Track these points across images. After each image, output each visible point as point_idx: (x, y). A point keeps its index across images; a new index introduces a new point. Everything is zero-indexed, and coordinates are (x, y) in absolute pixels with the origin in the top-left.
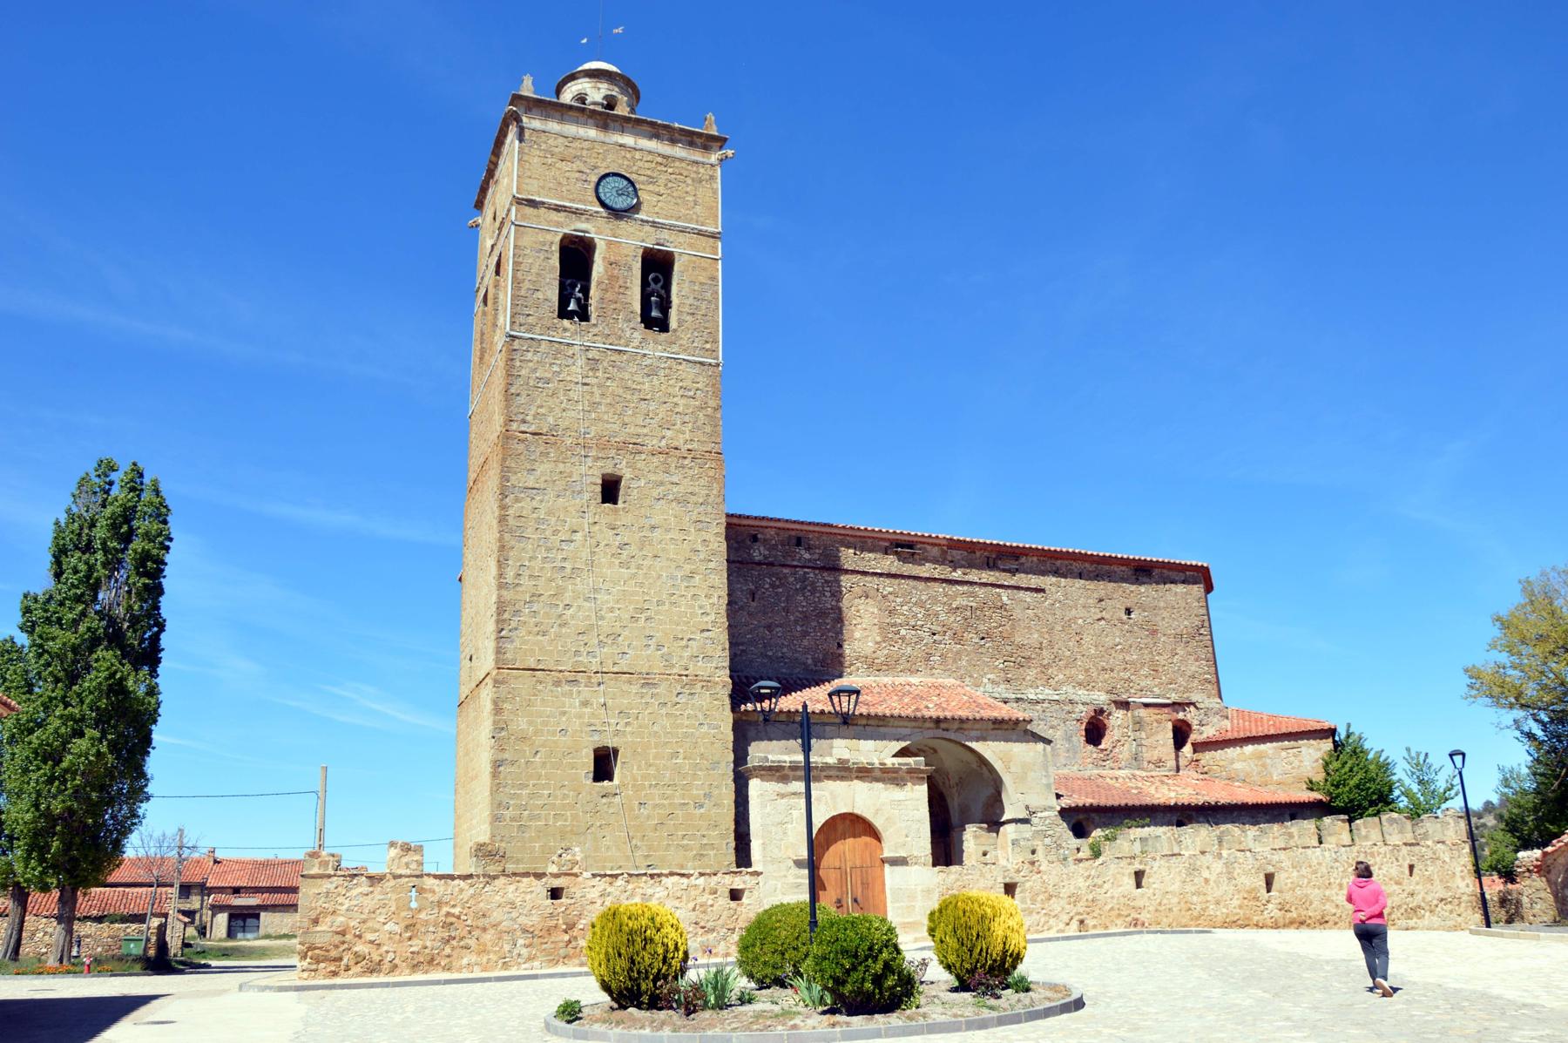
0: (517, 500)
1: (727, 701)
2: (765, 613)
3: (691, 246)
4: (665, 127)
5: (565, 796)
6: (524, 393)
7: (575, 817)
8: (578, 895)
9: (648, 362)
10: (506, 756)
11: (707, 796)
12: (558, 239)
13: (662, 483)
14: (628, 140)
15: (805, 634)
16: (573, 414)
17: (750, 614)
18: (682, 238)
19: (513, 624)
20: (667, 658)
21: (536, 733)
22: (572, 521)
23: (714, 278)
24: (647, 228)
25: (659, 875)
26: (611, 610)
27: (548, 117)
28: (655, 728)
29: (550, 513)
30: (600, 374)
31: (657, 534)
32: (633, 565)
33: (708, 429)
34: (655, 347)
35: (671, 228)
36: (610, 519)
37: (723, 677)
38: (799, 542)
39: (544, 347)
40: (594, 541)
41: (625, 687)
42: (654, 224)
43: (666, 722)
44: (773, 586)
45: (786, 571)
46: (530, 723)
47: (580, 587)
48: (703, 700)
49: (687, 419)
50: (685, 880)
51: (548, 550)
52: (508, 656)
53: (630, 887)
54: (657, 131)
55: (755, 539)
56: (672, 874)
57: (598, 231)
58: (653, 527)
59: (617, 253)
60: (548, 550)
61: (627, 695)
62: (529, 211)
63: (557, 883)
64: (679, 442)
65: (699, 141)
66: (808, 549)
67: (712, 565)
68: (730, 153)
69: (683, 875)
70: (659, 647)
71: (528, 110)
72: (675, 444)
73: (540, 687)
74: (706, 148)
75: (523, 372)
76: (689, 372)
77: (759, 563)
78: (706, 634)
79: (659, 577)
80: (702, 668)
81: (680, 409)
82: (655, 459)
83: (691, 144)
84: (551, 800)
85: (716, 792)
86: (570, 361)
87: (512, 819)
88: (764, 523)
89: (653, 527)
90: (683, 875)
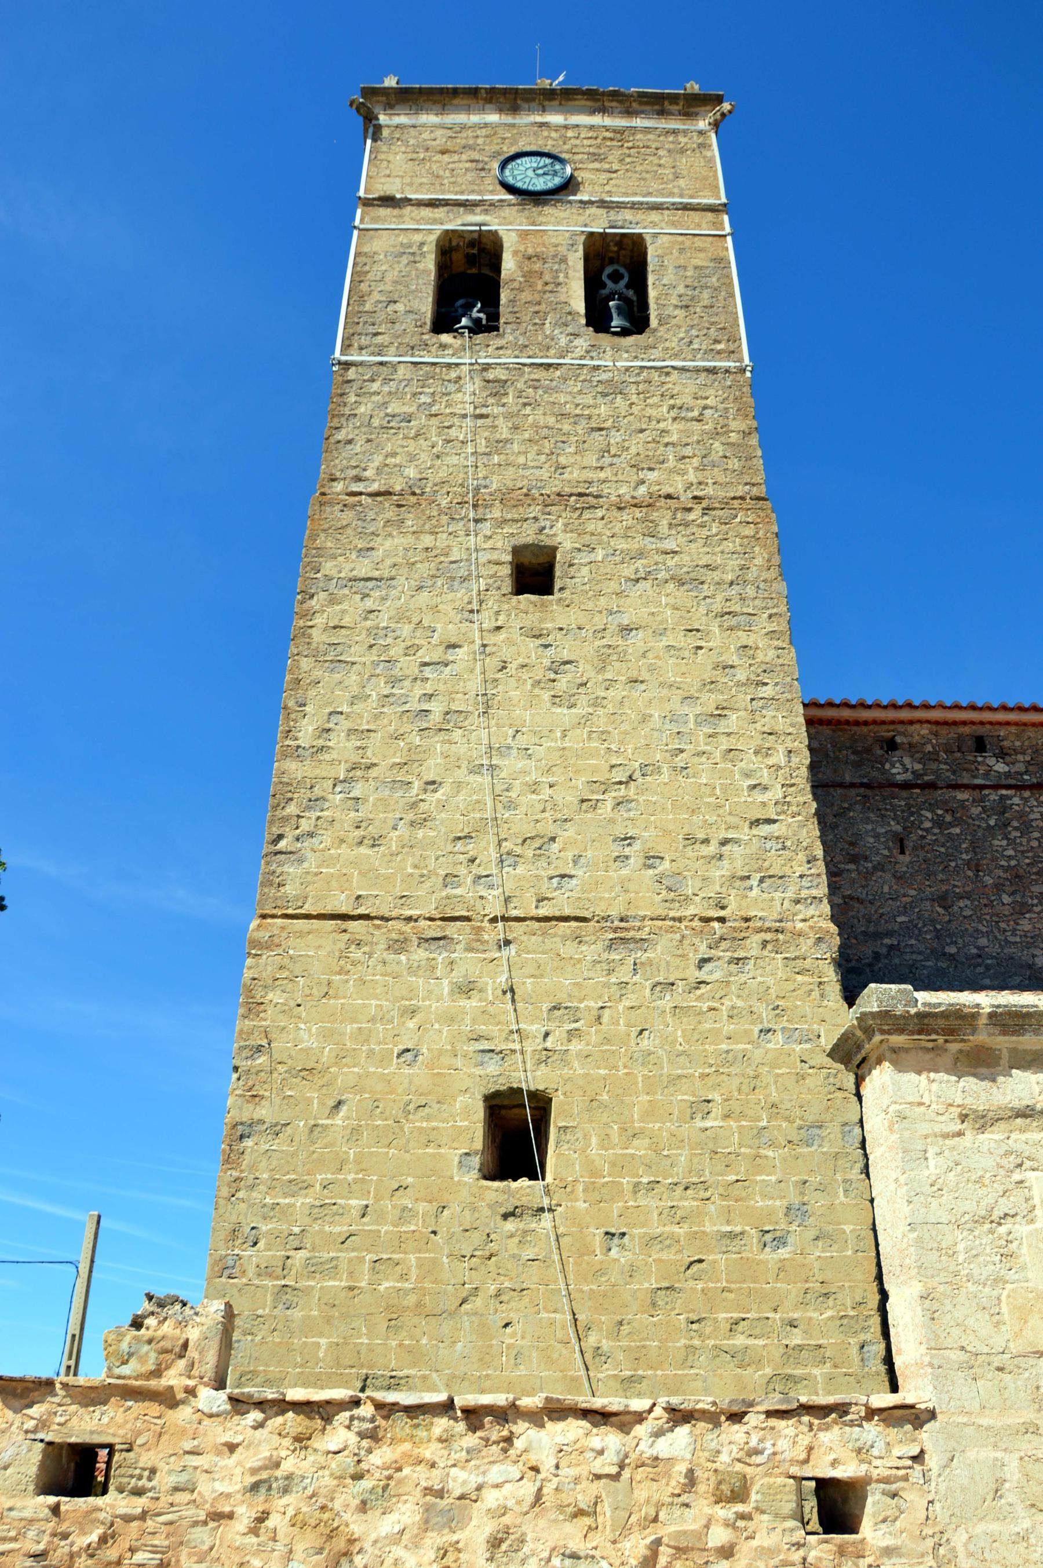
0: (333, 601)
1: (831, 975)
2: (930, 874)
3: (673, 224)
4: (615, 95)
5: (405, 1214)
6: (360, 441)
7: (429, 1269)
8: (165, 1480)
9: (604, 377)
10: (263, 1112)
11: (796, 1212)
12: (433, 238)
13: (641, 554)
14: (556, 119)
15: (1022, 909)
16: (454, 460)
17: (899, 878)
18: (654, 216)
19: (305, 825)
20: (671, 887)
21: (339, 1058)
22: (446, 628)
23: (721, 261)
24: (593, 210)
25: (504, 1414)
26: (534, 788)
27: (420, 110)
28: (645, 1043)
29: (401, 617)
30: (510, 399)
31: (637, 639)
32: (583, 700)
33: (734, 464)
34: (618, 355)
35: (633, 206)
36: (531, 620)
37: (816, 918)
38: (980, 745)
39: (401, 370)
40: (492, 663)
41: (569, 949)
42: (603, 204)
43: (677, 1029)
44: (939, 823)
45: (962, 795)
46: (327, 1035)
47: (461, 749)
48: (769, 973)
49: (688, 451)
50: (610, 1439)
51: (394, 681)
52: (290, 889)
53: (380, 1457)
54: (598, 100)
55: (891, 745)
56: (557, 1411)
57: (510, 226)
58: (626, 630)
59: (544, 252)
60: (394, 681)
61: (569, 969)
62: (383, 212)
63: (84, 1426)
64: (676, 486)
65: (674, 108)
66: (1002, 755)
67: (767, 691)
69: (600, 1417)
70: (651, 859)
71: (389, 106)
72: (667, 489)
73: (357, 954)
74: (688, 114)
75: (362, 409)
76: (685, 389)
77: (906, 786)
78: (765, 829)
79: (645, 719)
80: (762, 903)
81: (674, 438)
82: (625, 515)
83: (662, 113)
84: (368, 1225)
85: (818, 1202)
86: (452, 387)
87: (265, 1271)
88: (905, 714)
89: (626, 630)
90: (600, 1417)
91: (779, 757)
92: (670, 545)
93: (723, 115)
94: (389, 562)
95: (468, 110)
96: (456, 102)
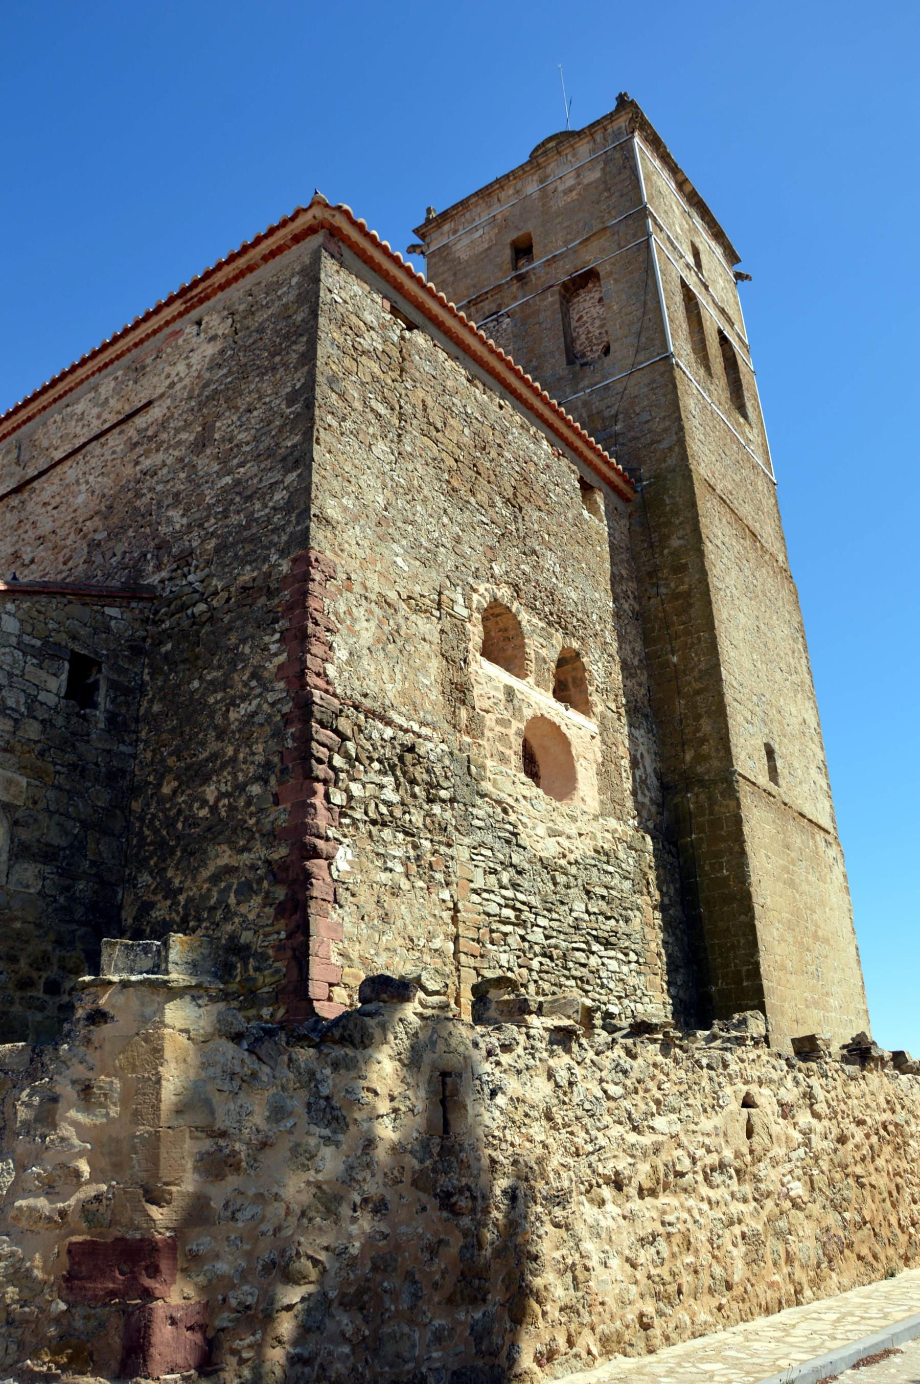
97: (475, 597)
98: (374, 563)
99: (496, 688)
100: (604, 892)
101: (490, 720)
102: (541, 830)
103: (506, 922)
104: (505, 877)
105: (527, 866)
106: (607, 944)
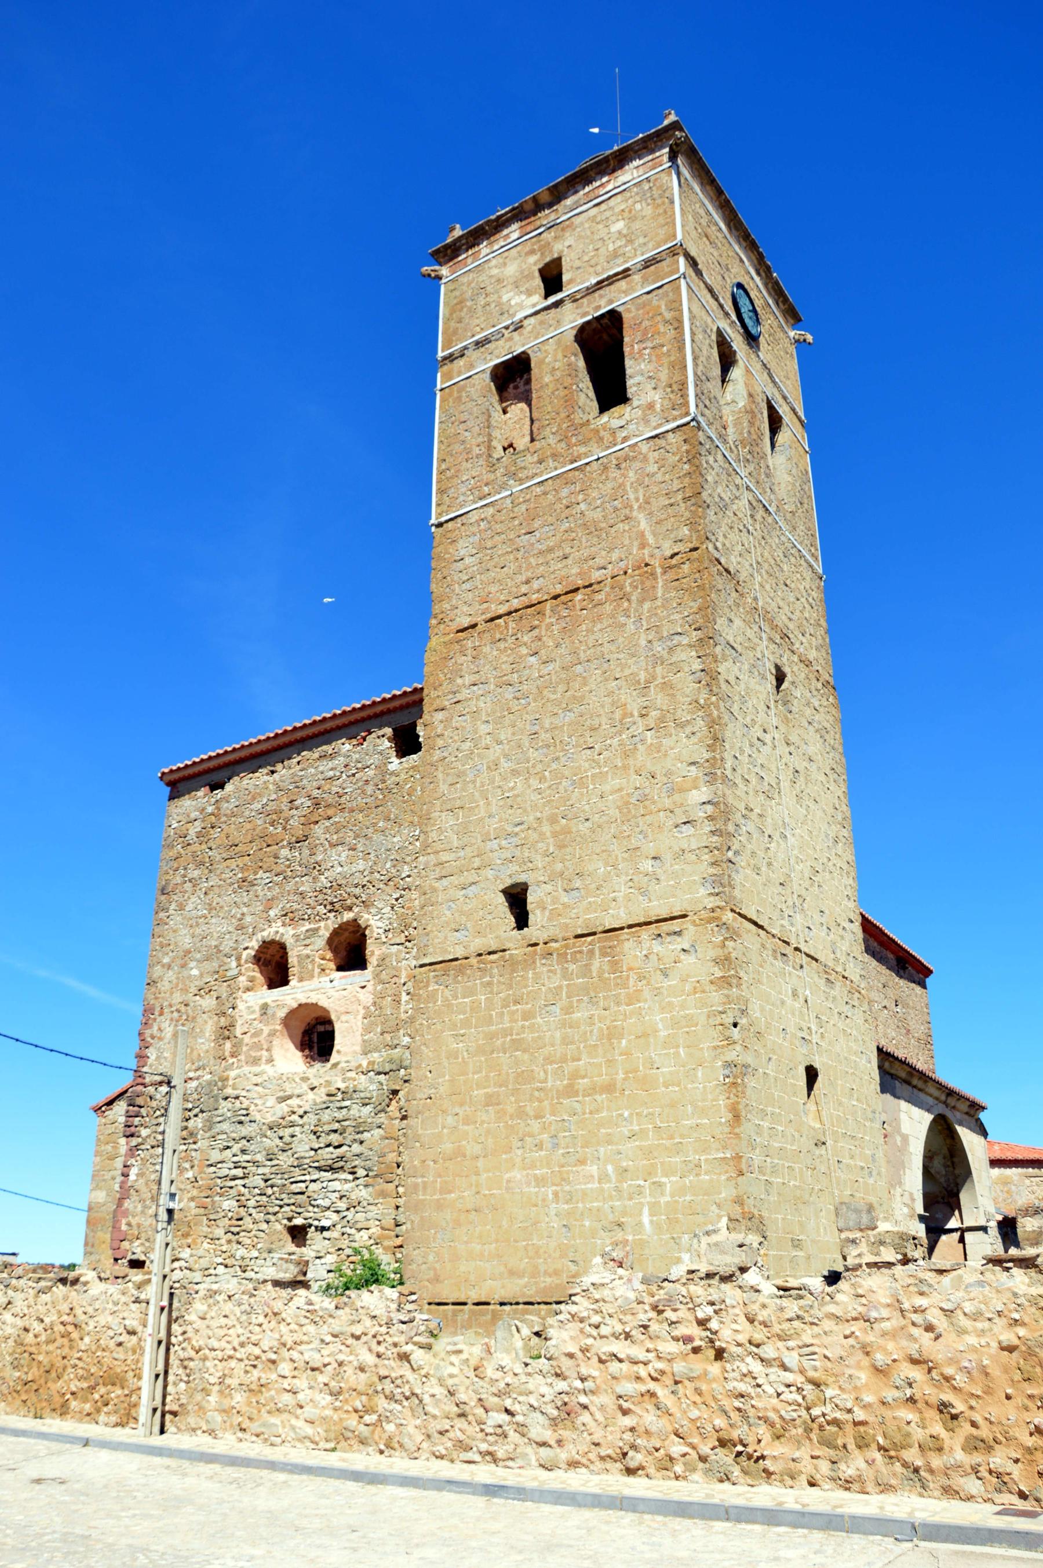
46: (762, 1009)
68: (810, 338)
91: (851, 881)
92: (817, 704)
93: (805, 340)
94: (739, 639)
95: (711, 200)
96: (708, 188)
97: (245, 954)
98: (177, 985)
99: (253, 1012)
100: (336, 1126)
101: (247, 1039)
102: (271, 1101)
103: (234, 1178)
104: (236, 1148)
105: (253, 1134)
106: (331, 1169)
